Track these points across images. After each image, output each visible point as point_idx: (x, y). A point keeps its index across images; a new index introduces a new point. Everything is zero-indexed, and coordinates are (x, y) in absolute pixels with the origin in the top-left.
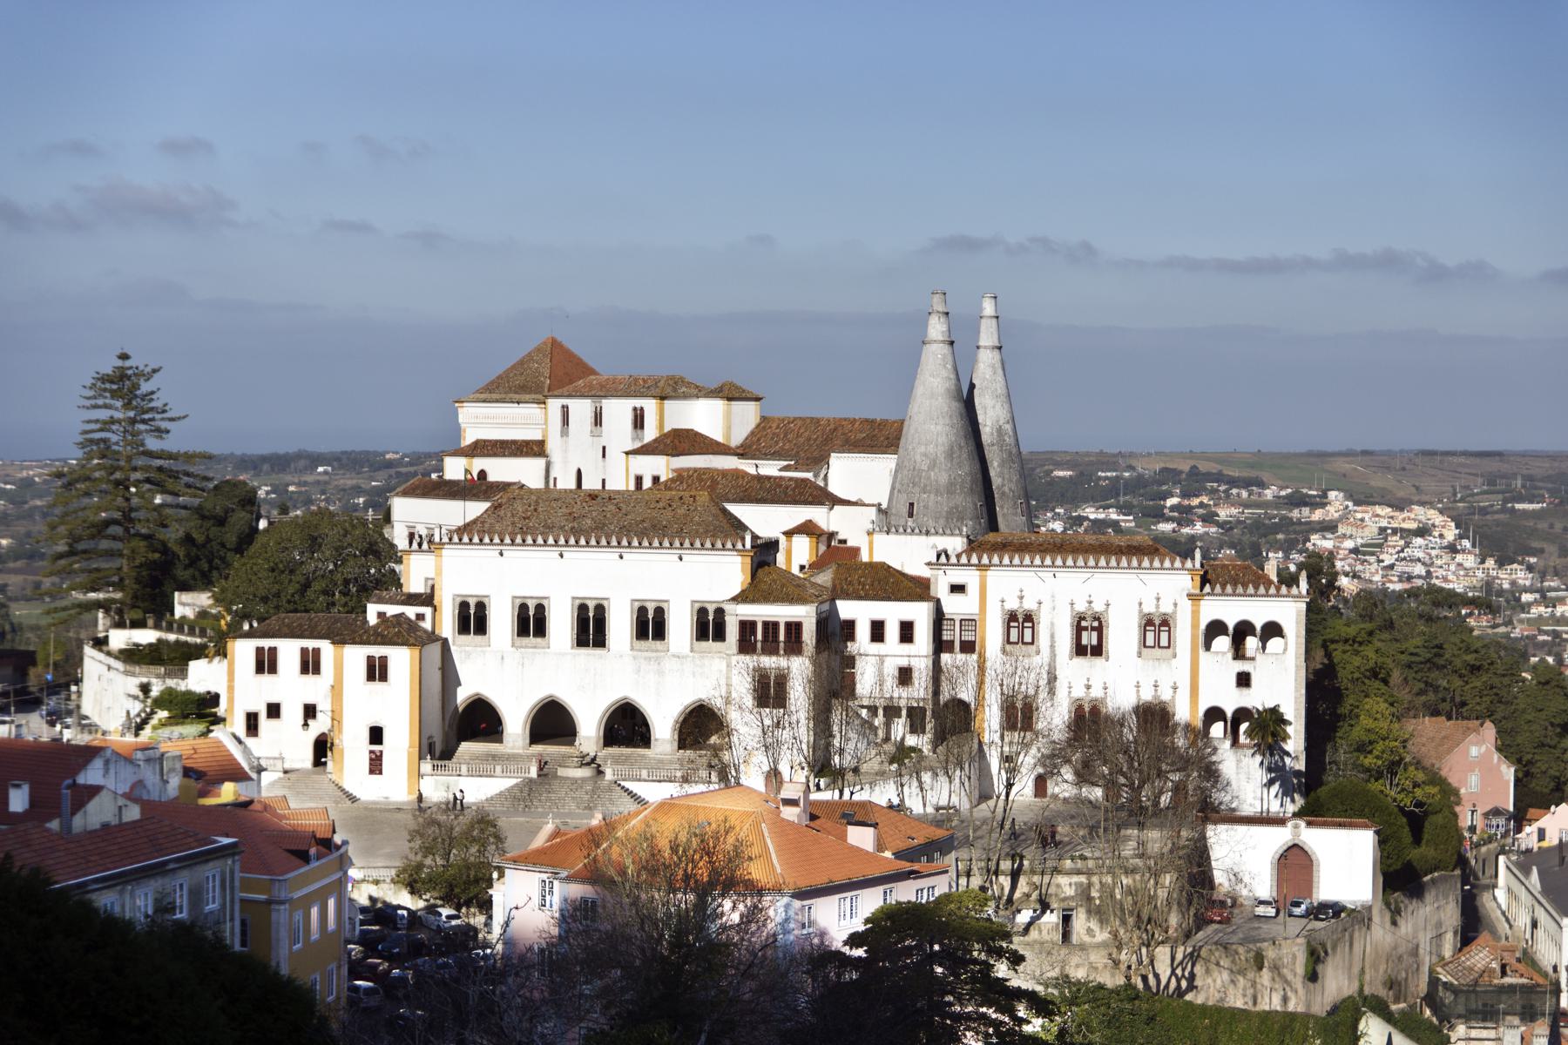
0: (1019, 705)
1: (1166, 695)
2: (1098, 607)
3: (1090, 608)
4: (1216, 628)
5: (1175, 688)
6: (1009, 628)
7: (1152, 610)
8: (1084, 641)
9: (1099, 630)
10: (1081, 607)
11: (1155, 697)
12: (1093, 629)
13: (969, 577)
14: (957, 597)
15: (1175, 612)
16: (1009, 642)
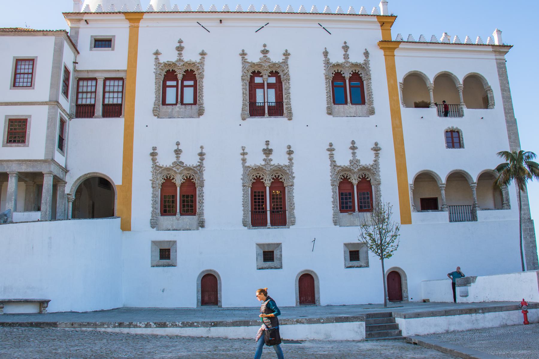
0: (178, 181)
1: (366, 159)
2: (276, 57)
3: (267, 60)
4: (415, 79)
5: (376, 149)
6: (165, 87)
7: (341, 60)
8: (259, 99)
9: (278, 87)
10: (255, 57)
11: (355, 162)
12: (270, 86)
13: (119, 31)
14: (103, 53)
15: (367, 63)
16: (164, 103)
